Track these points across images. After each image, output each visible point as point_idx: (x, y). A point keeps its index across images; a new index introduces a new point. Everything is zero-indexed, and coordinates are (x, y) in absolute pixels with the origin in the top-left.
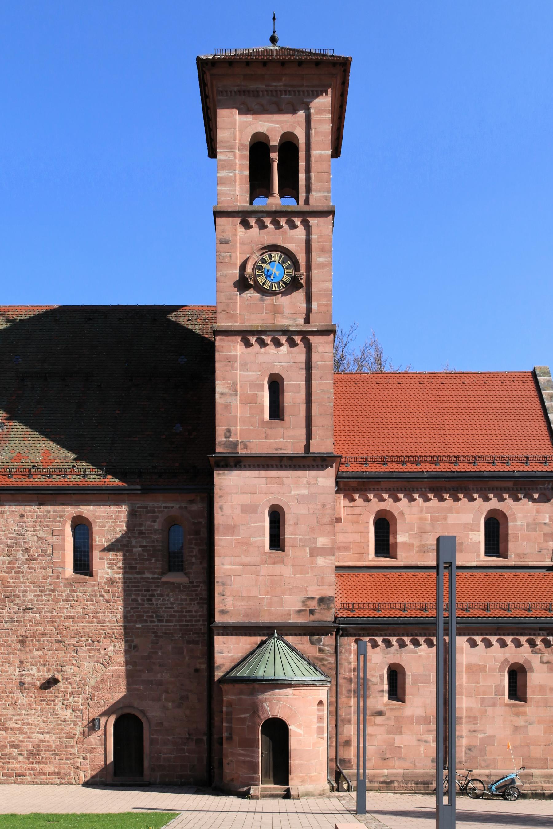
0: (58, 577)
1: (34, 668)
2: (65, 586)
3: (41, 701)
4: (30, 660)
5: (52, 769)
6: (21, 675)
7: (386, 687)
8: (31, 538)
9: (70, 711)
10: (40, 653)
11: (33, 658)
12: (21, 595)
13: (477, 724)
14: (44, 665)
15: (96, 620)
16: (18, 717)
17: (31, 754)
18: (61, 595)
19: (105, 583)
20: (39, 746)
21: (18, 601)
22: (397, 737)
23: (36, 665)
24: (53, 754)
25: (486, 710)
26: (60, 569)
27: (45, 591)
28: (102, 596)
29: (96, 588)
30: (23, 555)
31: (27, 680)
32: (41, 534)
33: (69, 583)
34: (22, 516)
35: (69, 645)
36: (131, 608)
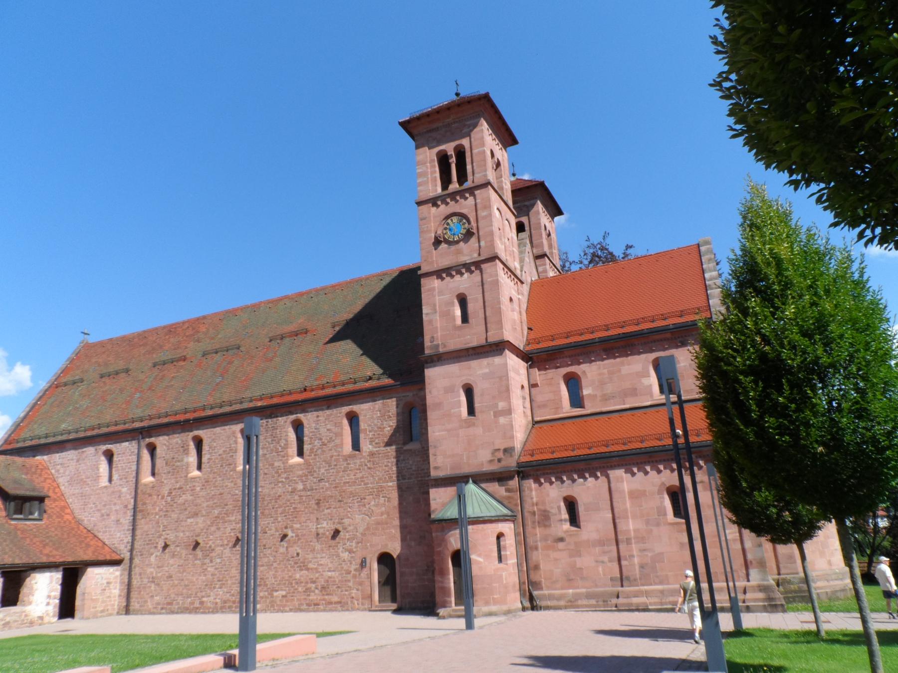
0: (339, 455)
1: (325, 523)
3: (330, 546)
4: (323, 517)
5: (335, 599)
6: (317, 528)
7: (565, 515)
8: (323, 430)
9: (347, 553)
10: (329, 511)
11: (324, 515)
12: (317, 470)
14: (331, 520)
15: (362, 483)
16: (315, 560)
17: (323, 588)
18: (341, 468)
19: (368, 456)
20: (327, 581)
21: (315, 475)
23: (325, 520)
24: (337, 587)
25: (651, 530)
26: (340, 450)
27: (331, 466)
28: (366, 465)
29: (362, 460)
30: (318, 443)
31: (321, 531)
32: (329, 427)
33: (347, 458)
34: (318, 416)
35: (346, 503)
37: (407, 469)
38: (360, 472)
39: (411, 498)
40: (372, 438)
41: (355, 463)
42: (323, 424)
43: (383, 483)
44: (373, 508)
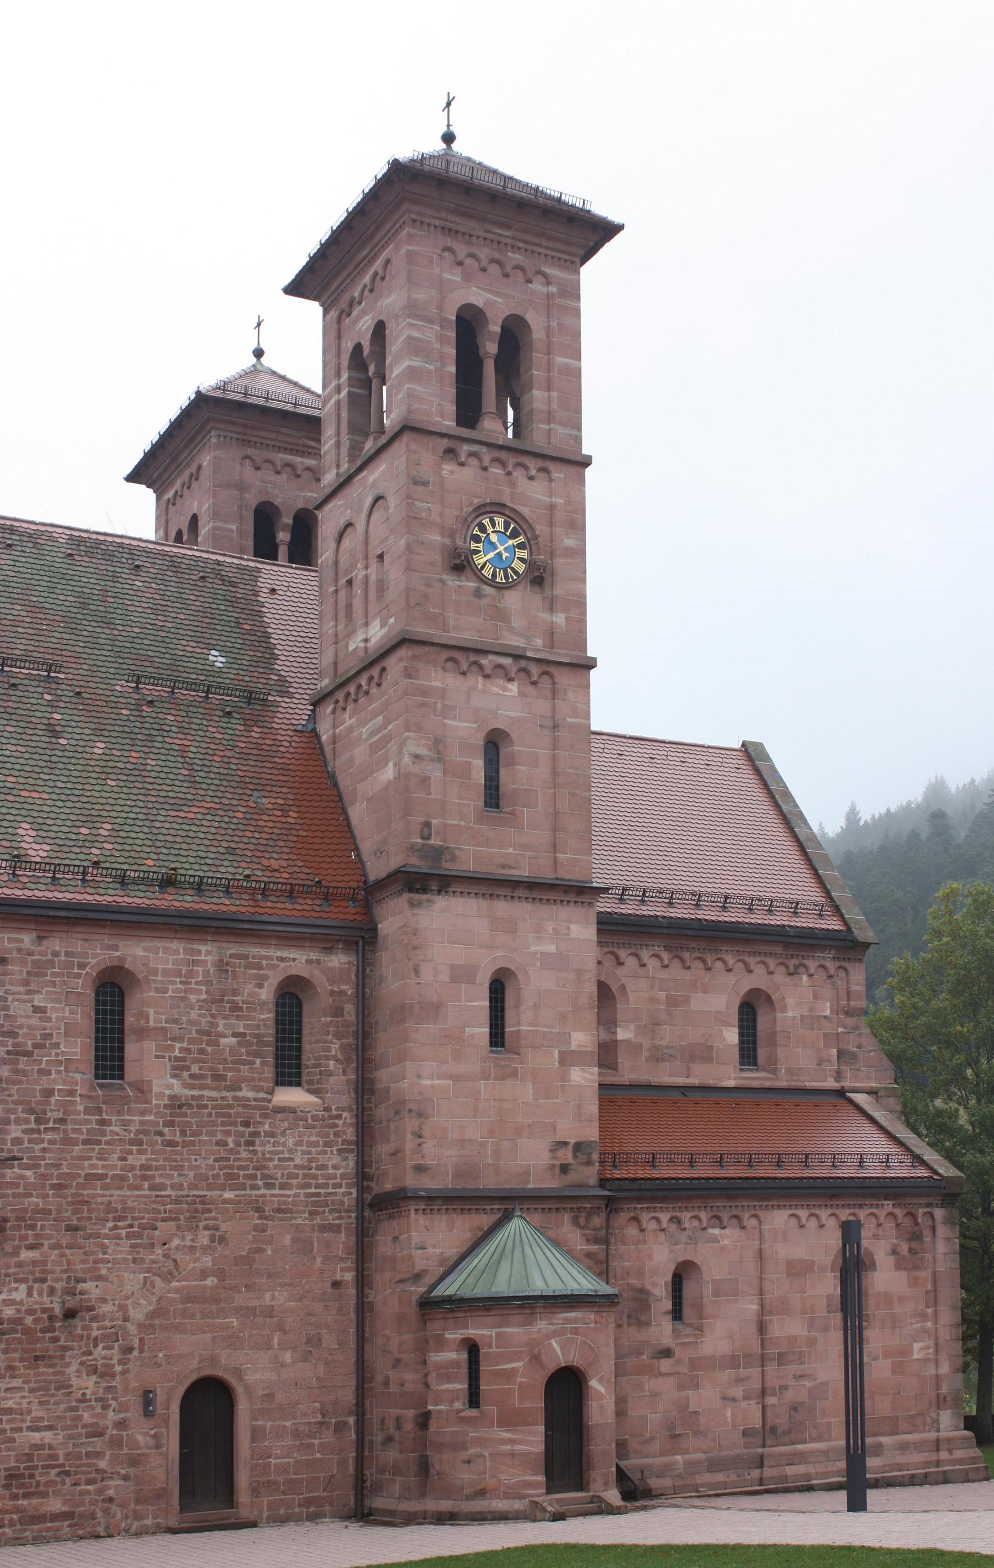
1: (23, 1287)
2: (87, 1111)
11: (20, 1265)
13: (804, 1363)
15: (146, 1184)
19: (166, 1106)
22: (692, 1394)
27: (47, 1122)
28: (161, 1134)
36: (215, 1160)
37: (279, 1160)
38: (140, 1152)
39: (287, 1240)
40: (184, 1059)
41: (125, 1124)
42: (22, 989)
43: (210, 1187)
44: (178, 1256)
